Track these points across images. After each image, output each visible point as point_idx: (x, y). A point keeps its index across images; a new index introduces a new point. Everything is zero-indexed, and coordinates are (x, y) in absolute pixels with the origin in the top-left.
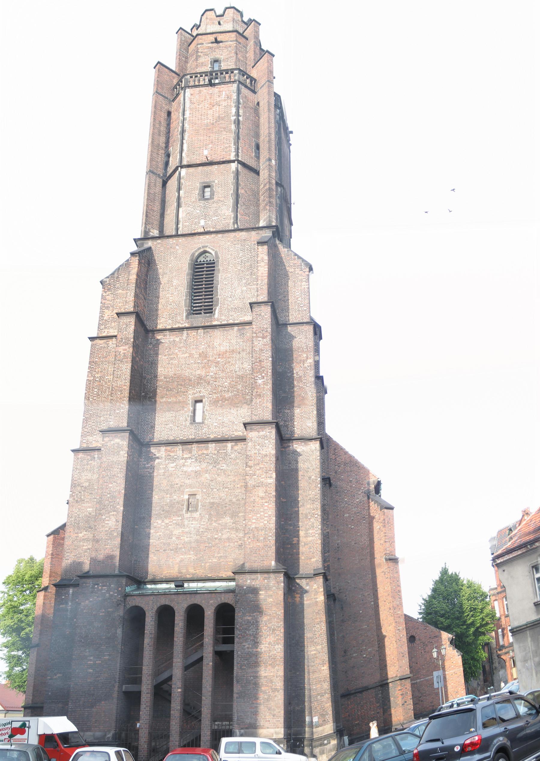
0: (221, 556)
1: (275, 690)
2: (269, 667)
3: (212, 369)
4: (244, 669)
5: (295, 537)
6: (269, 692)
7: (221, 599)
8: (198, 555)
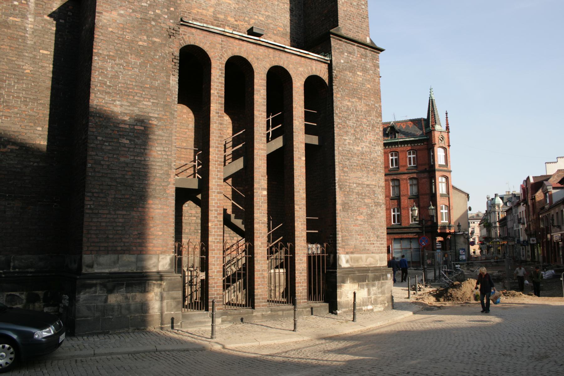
0: (268, 16)
1: (377, 204)
2: (371, 173)
4: (347, 172)
6: (372, 206)
7: (312, 69)
8: (241, 4)
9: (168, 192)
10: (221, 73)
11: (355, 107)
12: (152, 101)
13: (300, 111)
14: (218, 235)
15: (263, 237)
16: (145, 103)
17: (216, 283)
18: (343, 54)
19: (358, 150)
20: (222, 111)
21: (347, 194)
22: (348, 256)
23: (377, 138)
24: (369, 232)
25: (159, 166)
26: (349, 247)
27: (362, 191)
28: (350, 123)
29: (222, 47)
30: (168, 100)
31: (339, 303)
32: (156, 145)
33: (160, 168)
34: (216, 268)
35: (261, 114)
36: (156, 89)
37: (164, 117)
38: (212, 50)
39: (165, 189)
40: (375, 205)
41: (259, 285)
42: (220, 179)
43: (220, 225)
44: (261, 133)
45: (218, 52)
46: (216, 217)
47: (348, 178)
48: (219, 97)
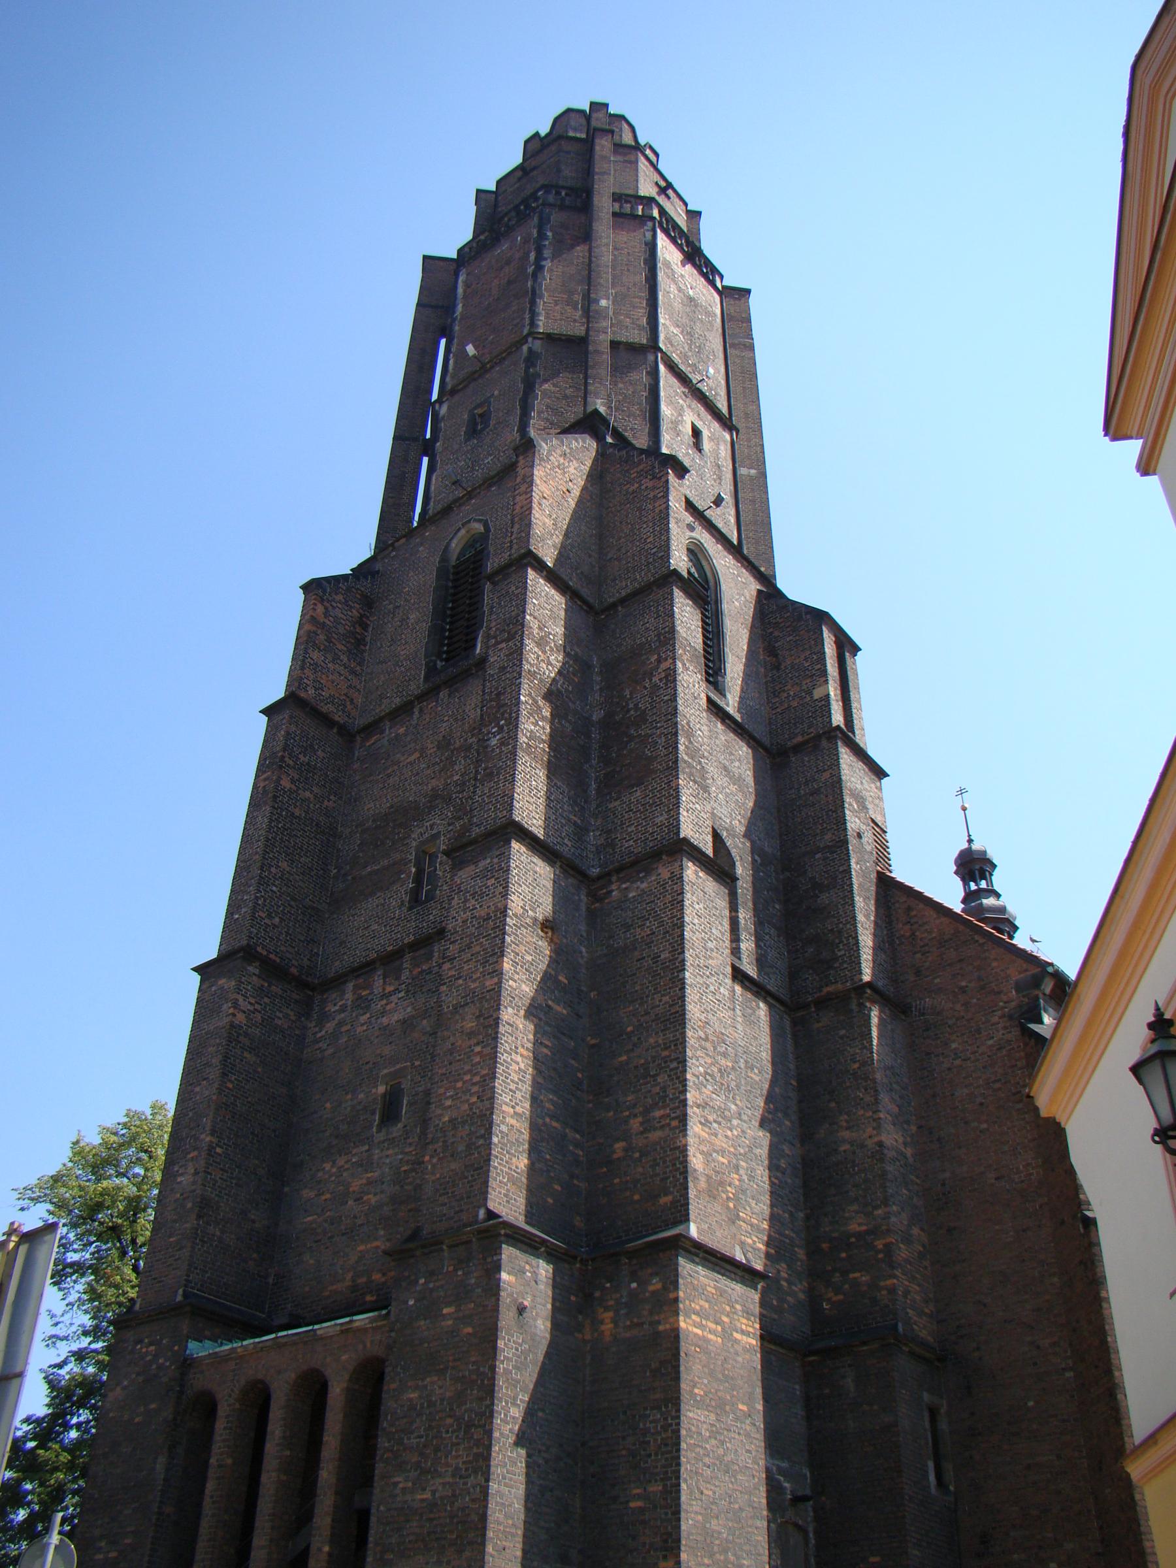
3: (456, 768)
5: (618, 1140)
19: (423, 1500)
23: (476, 1454)
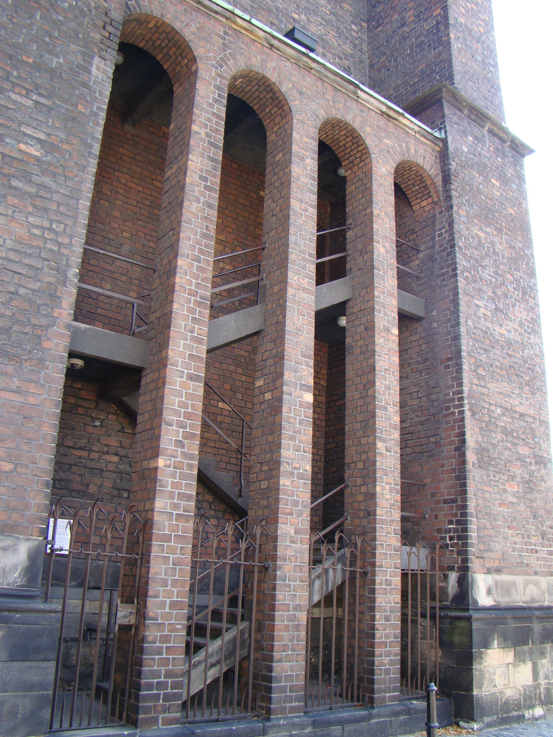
2: (527, 389)
7: (408, 149)
9: (46, 344)
10: (219, 95)
11: (493, 244)
12: (35, 97)
13: (387, 226)
14: (181, 496)
15: (300, 514)
16: (14, 97)
17: (165, 639)
18: (466, 136)
19: (501, 335)
20: (215, 176)
21: (486, 428)
22: (490, 579)
24: (528, 522)
25: (30, 266)
26: (492, 555)
27: (512, 427)
28: (486, 274)
29: (224, 44)
30: (80, 107)
31: (478, 699)
32: (31, 209)
33: (31, 273)
34: (169, 594)
35: (306, 211)
36: (53, 73)
37: (65, 146)
38: (202, 43)
39: (39, 337)
40: (536, 463)
41: (285, 648)
42: (198, 341)
43: (190, 466)
44: (303, 252)
45: (214, 52)
46: (180, 444)
47: (485, 391)
48: (210, 143)
